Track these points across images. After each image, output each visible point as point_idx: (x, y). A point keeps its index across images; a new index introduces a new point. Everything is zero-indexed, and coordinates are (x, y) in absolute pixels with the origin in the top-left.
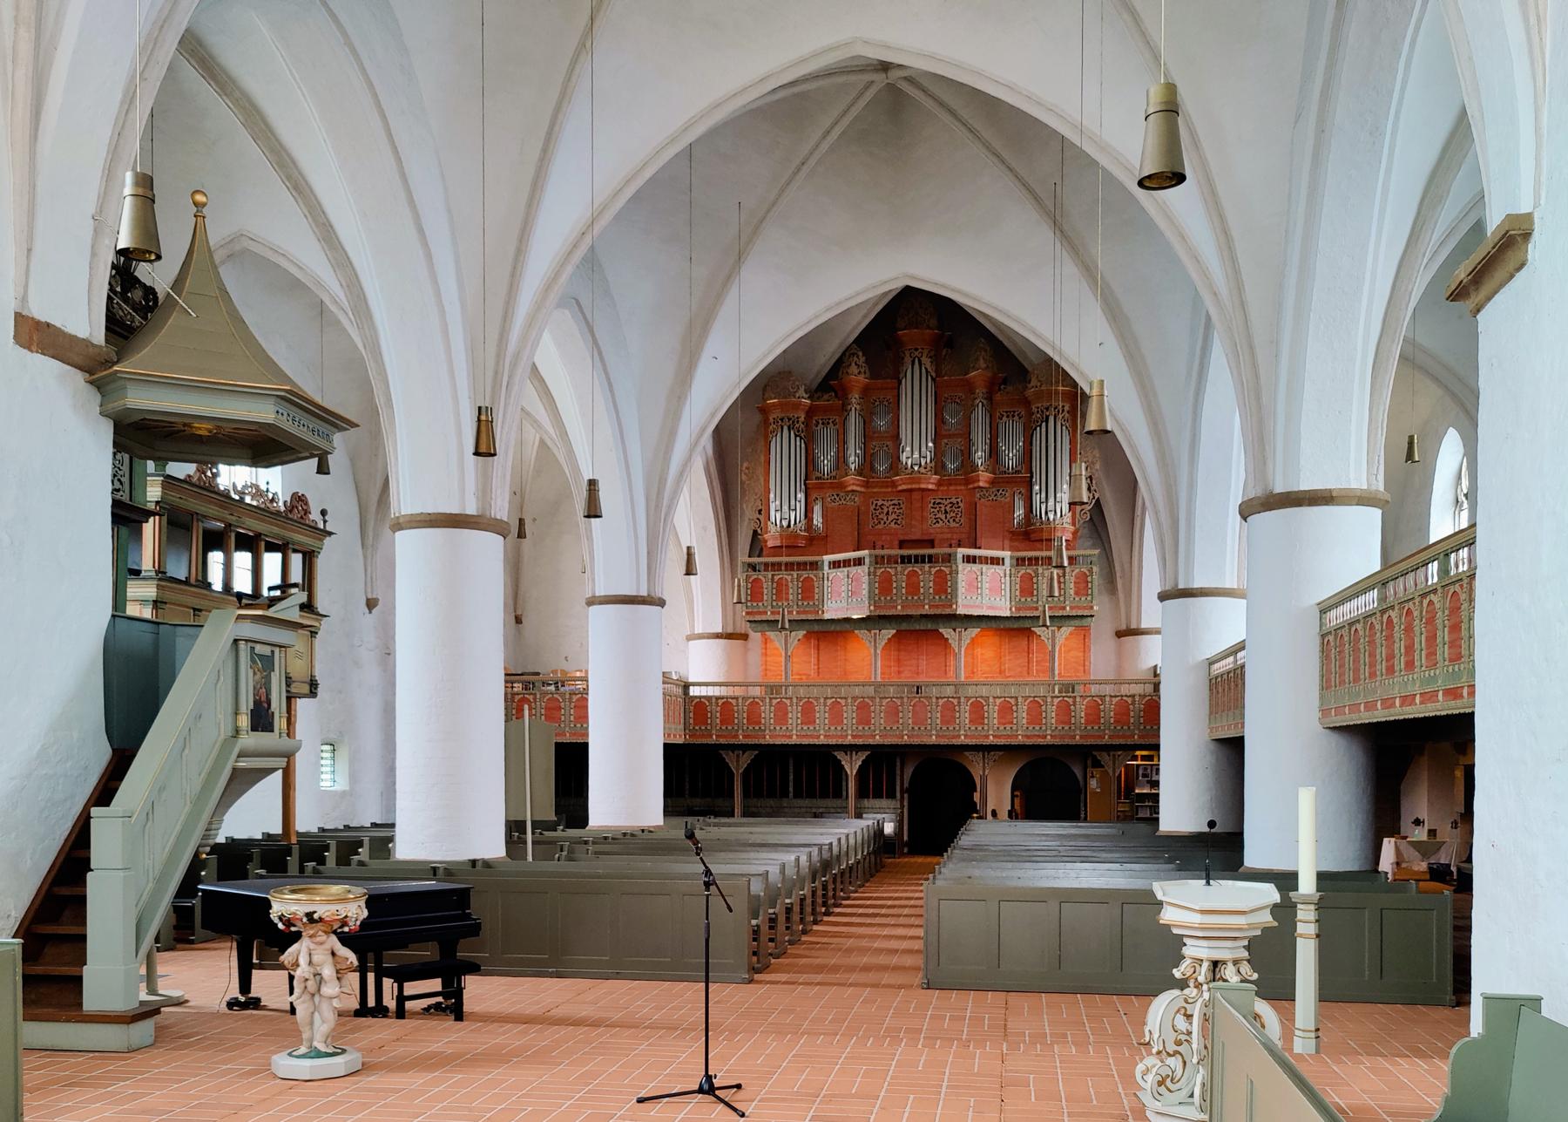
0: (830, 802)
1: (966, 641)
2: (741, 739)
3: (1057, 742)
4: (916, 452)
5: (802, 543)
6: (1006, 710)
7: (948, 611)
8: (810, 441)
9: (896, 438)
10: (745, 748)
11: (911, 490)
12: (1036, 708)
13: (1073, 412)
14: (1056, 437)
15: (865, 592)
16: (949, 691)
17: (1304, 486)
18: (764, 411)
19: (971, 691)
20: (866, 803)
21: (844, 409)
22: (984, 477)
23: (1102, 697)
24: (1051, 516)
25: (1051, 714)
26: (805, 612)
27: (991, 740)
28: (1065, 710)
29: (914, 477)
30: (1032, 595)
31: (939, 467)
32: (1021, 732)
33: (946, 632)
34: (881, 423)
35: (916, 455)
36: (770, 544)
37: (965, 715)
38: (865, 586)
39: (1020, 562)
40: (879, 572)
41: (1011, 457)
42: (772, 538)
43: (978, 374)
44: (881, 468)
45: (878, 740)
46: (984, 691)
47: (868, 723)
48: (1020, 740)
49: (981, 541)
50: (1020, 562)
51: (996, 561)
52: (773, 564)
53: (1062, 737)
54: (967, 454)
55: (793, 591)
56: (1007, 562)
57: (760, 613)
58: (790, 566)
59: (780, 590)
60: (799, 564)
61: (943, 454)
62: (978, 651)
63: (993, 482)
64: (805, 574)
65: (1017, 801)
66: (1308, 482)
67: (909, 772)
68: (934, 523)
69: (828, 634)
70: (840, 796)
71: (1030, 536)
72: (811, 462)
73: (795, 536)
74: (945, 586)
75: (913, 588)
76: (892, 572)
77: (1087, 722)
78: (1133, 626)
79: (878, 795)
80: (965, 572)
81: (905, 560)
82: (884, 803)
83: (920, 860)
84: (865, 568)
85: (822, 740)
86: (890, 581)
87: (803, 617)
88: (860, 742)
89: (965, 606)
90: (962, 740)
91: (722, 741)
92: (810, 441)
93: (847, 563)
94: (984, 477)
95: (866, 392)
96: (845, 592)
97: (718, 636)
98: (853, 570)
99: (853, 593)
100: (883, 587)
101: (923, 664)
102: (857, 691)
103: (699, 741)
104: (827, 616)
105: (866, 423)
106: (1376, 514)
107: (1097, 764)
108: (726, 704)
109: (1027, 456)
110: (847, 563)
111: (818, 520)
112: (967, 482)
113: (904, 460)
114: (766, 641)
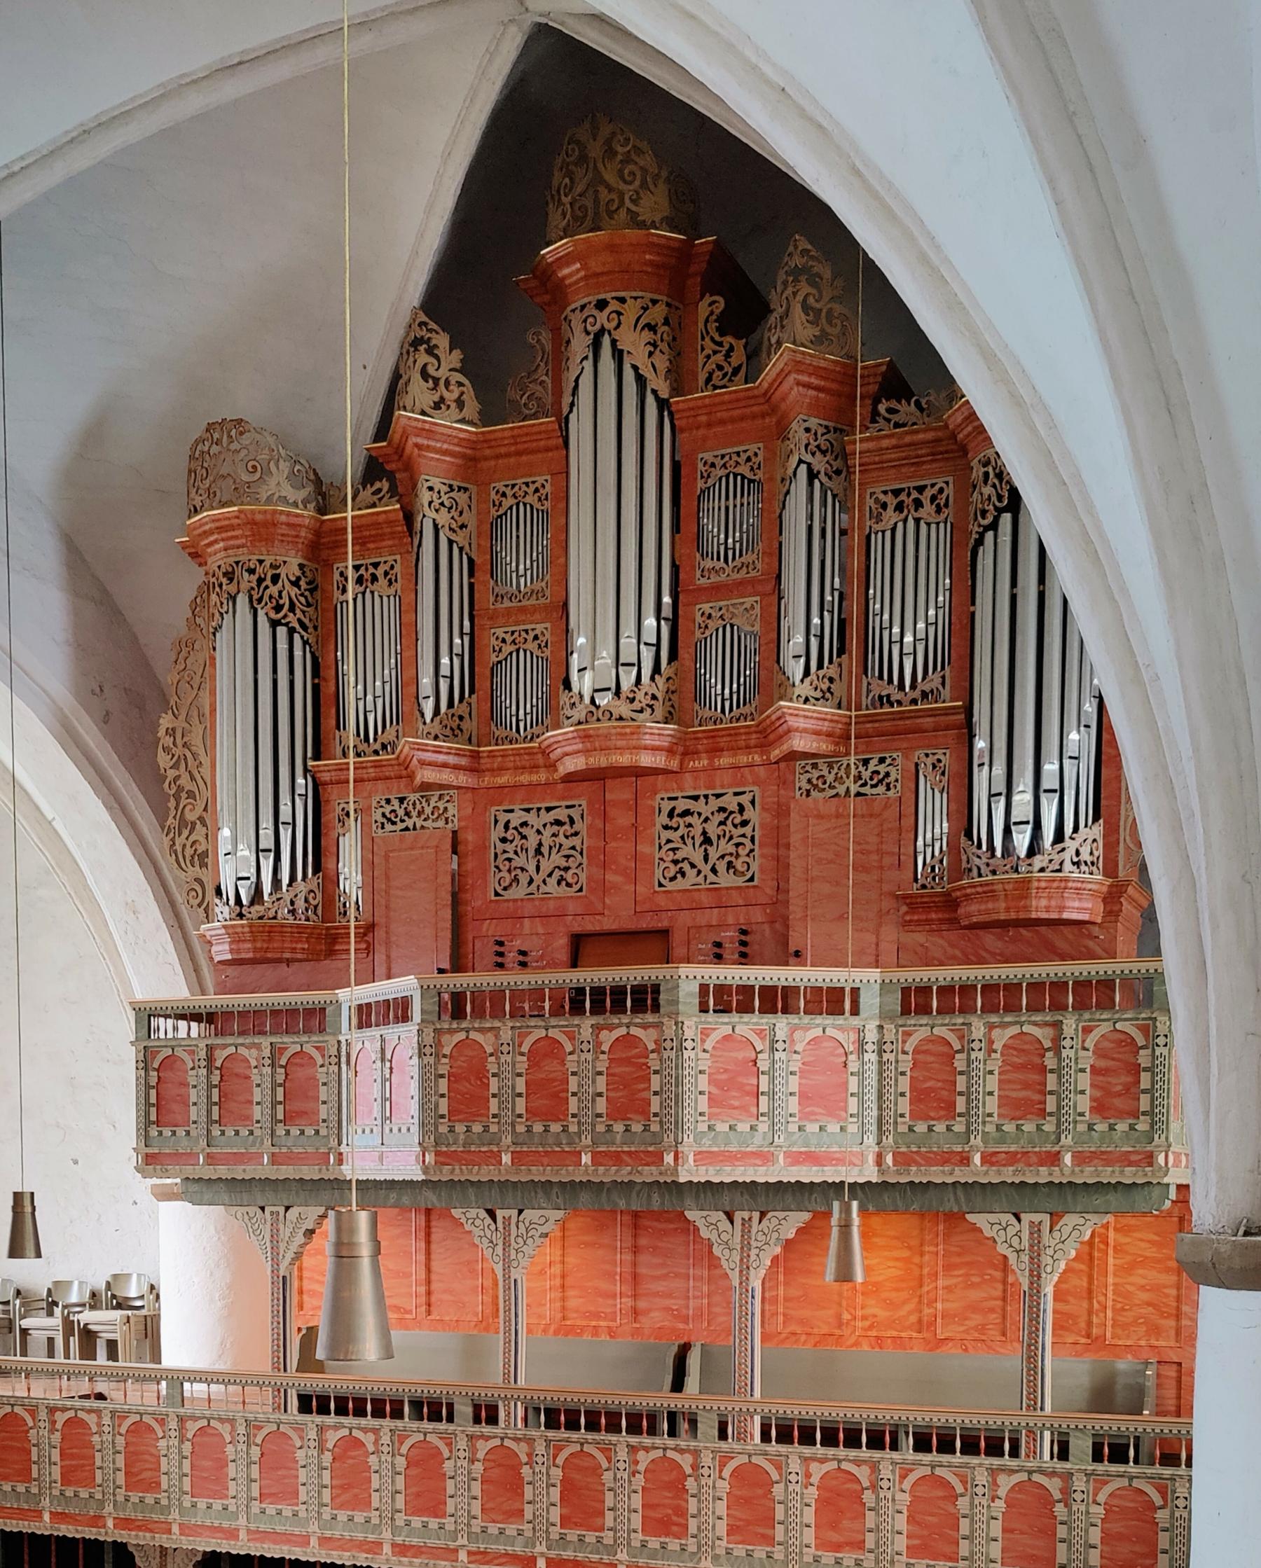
7: (649, 1174)
15: (414, 1107)
22: (805, 719)
33: (707, 1221)
34: (519, 567)
35: (606, 656)
38: (413, 1088)
39: (915, 1001)
49: (804, 935)
50: (915, 1001)
51: (832, 1001)
56: (870, 1001)
58: (252, 1022)
64: (292, 1044)
68: (672, 869)
76: (487, 1042)
86: (481, 1076)
87: (286, 1172)
89: (703, 1157)
98: (393, 1032)
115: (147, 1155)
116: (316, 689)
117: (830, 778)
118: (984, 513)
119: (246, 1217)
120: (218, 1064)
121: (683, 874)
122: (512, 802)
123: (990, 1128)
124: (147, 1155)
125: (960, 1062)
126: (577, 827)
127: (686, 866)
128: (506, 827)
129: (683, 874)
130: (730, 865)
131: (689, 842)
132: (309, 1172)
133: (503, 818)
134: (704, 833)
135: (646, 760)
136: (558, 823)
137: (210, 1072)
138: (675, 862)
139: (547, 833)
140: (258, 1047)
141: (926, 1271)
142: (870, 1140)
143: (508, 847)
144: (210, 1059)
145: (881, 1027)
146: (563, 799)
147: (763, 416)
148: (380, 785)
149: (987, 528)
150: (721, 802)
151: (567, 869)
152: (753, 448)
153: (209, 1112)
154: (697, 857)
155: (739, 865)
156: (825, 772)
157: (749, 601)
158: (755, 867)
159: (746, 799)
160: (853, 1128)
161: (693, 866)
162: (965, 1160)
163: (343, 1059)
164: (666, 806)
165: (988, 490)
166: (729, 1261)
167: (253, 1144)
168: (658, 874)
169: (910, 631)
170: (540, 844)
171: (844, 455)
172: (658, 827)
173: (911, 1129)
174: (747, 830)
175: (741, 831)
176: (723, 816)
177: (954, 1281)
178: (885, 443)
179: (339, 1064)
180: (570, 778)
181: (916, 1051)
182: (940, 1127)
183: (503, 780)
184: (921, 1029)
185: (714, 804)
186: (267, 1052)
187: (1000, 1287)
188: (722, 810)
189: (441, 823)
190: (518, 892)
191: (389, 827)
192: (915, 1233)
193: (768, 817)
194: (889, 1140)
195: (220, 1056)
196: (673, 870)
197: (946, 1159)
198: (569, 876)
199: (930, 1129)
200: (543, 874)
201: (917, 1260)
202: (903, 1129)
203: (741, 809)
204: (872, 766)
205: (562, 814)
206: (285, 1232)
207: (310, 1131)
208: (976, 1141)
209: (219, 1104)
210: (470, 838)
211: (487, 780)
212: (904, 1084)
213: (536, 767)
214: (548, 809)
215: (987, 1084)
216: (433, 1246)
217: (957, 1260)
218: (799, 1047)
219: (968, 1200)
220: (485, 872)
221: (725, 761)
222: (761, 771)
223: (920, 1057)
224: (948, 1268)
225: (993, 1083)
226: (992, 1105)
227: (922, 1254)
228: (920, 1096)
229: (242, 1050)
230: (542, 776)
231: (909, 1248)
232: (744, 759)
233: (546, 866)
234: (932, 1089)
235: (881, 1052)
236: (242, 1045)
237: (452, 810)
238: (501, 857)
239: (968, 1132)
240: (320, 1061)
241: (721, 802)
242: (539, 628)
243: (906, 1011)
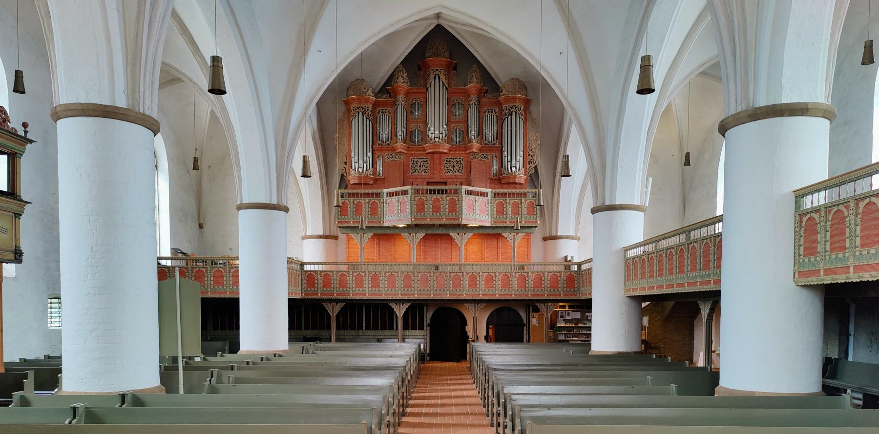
0: (388, 332)
1: (464, 242)
2: (335, 296)
3: (518, 298)
4: (437, 130)
5: (370, 182)
6: (490, 280)
7: (456, 222)
8: (374, 122)
9: (425, 123)
10: (337, 301)
11: (433, 153)
12: (506, 279)
14: (516, 126)
15: (409, 210)
16: (456, 269)
17: (785, 100)
19: (469, 269)
20: (407, 332)
21: (394, 104)
22: (476, 146)
23: (543, 273)
24: (514, 169)
25: (514, 282)
26: (372, 222)
27: (481, 297)
28: (523, 280)
29: (436, 145)
31: (450, 140)
32: (498, 293)
34: (417, 114)
35: (437, 132)
36: (352, 182)
37: (466, 283)
39: (496, 195)
40: (417, 199)
41: (491, 133)
42: (353, 178)
43: (473, 85)
44: (416, 139)
45: (416, 297)
46: (477, 269)
47: (410, 287)
48: (497, 297)
50: (496, 195)
51: (483, 194)
52: (354, 194)
53: (521, 295)
54: (466, 132)
55: (365, 210)
56: (489, 195)
57: (345, 222)
59: (358, 209)
60: (369, 194)
61: (452, 132)
62: (470, 247)
63: (480, 150)
64: (372, 200)
65: (491, 332)
66: (787, 98)
67: (430, 314)
69: (385, 236)
70: (392, 329)
71: (502, 180)
72: (375, 135)
73: (367, 177)
74: (455, 207)
75: (437, 209)
76: (425, 199)
77: (535, 287)
78: (554, 234)
79: (414, 328)
80: (466, 200)
81: (431, 192)
82: (417, 332)
83: (439, 364)
84: (409, 196)
85: (384, 297)
88: (406, 298)
90: (465, 297)
91: (324, 297)
92: (374, 122)
93: (397, 194)
94: (476, 146)
95: (407, 94)
96: (397, 211)
97: (320, 237)
98: (401, 197)
99: (401, 211)
100: (420, 207)
101: (439, 253)
102: (404, 268)
103: (310, 297)
104: (386, 225)
105: (408, 113)
106: (822, 126)
107: (537, 310)
108: (326, 275)
109: (500, 136)
110: (397, 194)
111: (379, 168)
112: (466, 149)
113: (429, 133)
114: (349, 239)
132: (375, 225)
135: (441, 150)
166: (458, 241)
169: (491, 133)
184: (498, 200)
190: (416, 174)
197: (502, 222)
215: (509, 209)
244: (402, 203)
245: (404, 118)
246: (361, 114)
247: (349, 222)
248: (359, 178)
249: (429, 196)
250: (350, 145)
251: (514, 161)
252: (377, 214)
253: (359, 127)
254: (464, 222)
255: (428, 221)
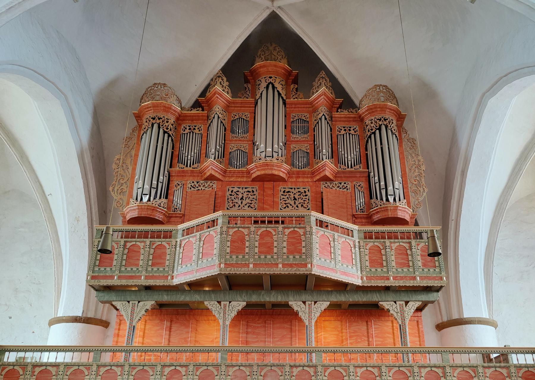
5: (159, 216)
13: (400, 127)
18: (138, 117)
24: (391, 199)
26: (153, 277)
30: (382, 265)
31: (290, 161)
35: (269, 149)
39: (368, 236)
40: (231, 231)
56: (356, 234)
57: (105, 277)
58: (145, 235)
62: (322, 335)
63: (337, 175)
64: (158, 242)
73: (154, 209)
93: (200, 227)
97: (76, 320)
104: (176, 281)
109: (364, 159)
110: (200, 227)
113: (258, 153)
115: (92, 276)
116: (172, 152)
117: (331, 186)
118: (372, 130)
119: (121, 305)
120: (128, 247)
121: (288, 207)
122: (234, 185)
123: (394, 270)
124: (92, 276)
125: (383, 252)
126: (254, 193)
127: (289, 205)
128: (232, 192)
129: (288, 207)
130: (302, 206)
131: (290, 199)
133: (231, 189)
134: (294, 197)
136: (249, 192)
137: (124, 249)
138: (286, 204)
139: (245, 194)
140: (144, 242)
141: (344, 338)
142: (359, 272)
143: (232, 197)
144: (125, 246)
145: (359, 242)
146: (251, 185)
147: (309, 108)
148: (191, 178)
149: (373, 133)
150: (299, 190)
151: (251, 204)
152: (306, 114)
153: (121, 262)
154: (292, 203)
155: (305, 205)
156: (329, 185)
157: (306, 145)
158: (309, 206)
159: (305, 190)
160: (354, 268)
161: (291, 205)
162: (388, 279)
163: (178, 246)
164: (283, 190)
165: (372, 125)
167: (138, 272)
168: (280, 206)
170: (243, 197)
171: (332, 117)
172: (280, 195)
173: (370, 270)
174: (307, 197)
175: (305, 197)
176: (300, 193)
177: (353, 341)
178: (342, 116)
179: (175, 248)
180: (254, 180)
181: (370, 249)
182: (379, 270)
183: (232, 179)
184: (371, 244)
185: (297, 190)
186: (148, 243)
187: (367, 342)
188: (299, 192)
189: (211, 189)
191: (192, 189)
192: (340, 326)
193: (313, 194)
194: (364, 273)
195: (129, 245)
196: (285, 206)
197: (382, 278)
198: (252, 205)
199: (376, 270)
200: (243, 204)
201: (341, 335)
202: (368, 270)
203: (305, 192)
204: (342, 184)
205: (250, 190)
206: (137, 310)
207: (161, 269)
208: (391, 273)
209: (126, 260)
210: (220, 193)
211: (227, 179)
212: (367, 258)
213: (243, 177)
214: (246, 188)
216: (172, 333)
217: (352, 334)
218: (340, 242)
219: (381, 297)
220: (224, 204)
221: (300, 180)
222: (311, 183)
223: (371, 251)
224: (350, 337)
225: (393, 258)
226: (394, 264)
227: (342, 333)
228: (372, 262)
229: (138, 243)
230: (245, 179)
231: (338, 331)
232: (306, 180)
233: (244, 202)
234: (375, 259)
235: (359, 249)
236: (138, 241)
237: (214, 186)
238: (230, 199)
239: (388, 271)
240: (168, 247)
241: (299, 190)
242: (245, 145)
243: (365, 238)
244: (206, 242)
245: (221, 140)
246: (156, 126)
247: (112, 277)
248: (140, 208)
249: (253, 228)
250: (134, 169)
251: (390, 188)
252: (163, 264)
253: (149, 143)
254: (316, 271)
255: (251, 269)
